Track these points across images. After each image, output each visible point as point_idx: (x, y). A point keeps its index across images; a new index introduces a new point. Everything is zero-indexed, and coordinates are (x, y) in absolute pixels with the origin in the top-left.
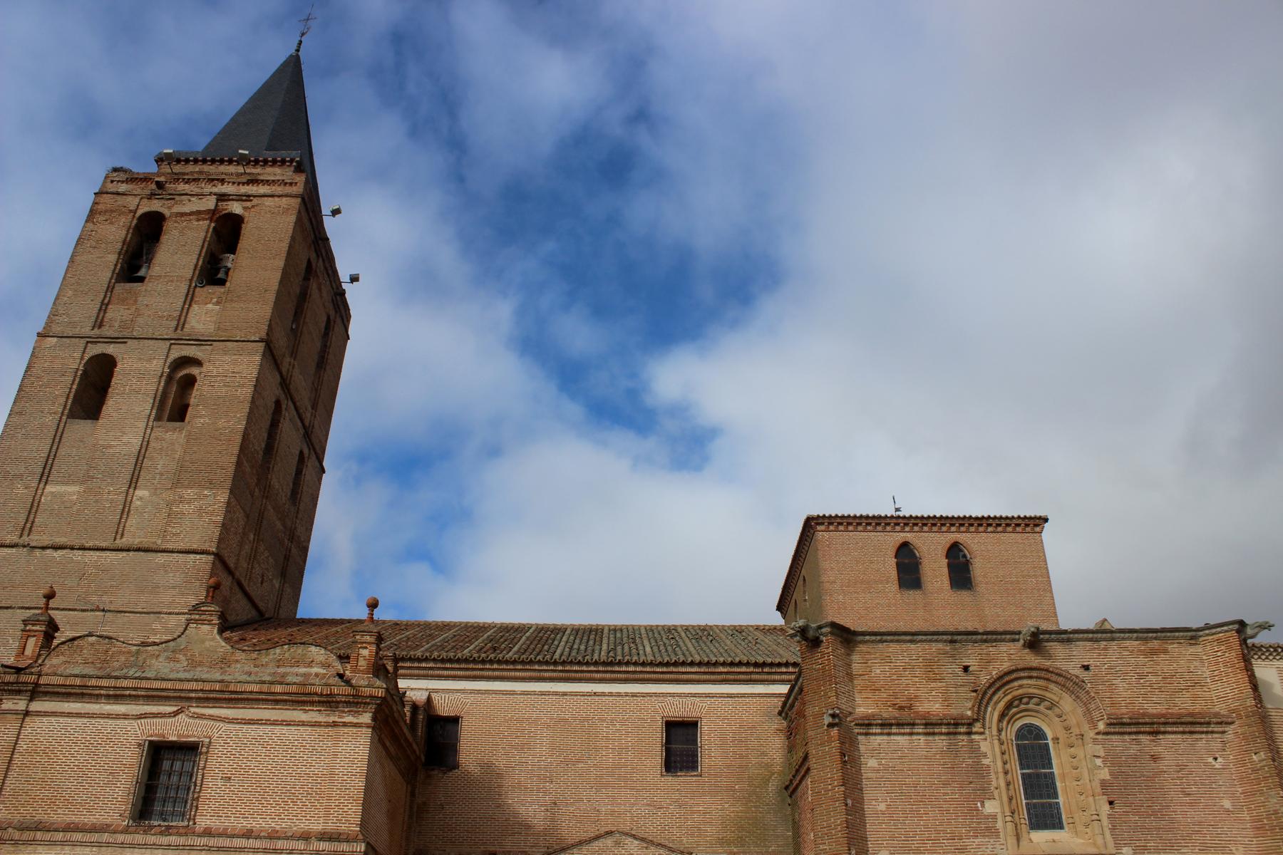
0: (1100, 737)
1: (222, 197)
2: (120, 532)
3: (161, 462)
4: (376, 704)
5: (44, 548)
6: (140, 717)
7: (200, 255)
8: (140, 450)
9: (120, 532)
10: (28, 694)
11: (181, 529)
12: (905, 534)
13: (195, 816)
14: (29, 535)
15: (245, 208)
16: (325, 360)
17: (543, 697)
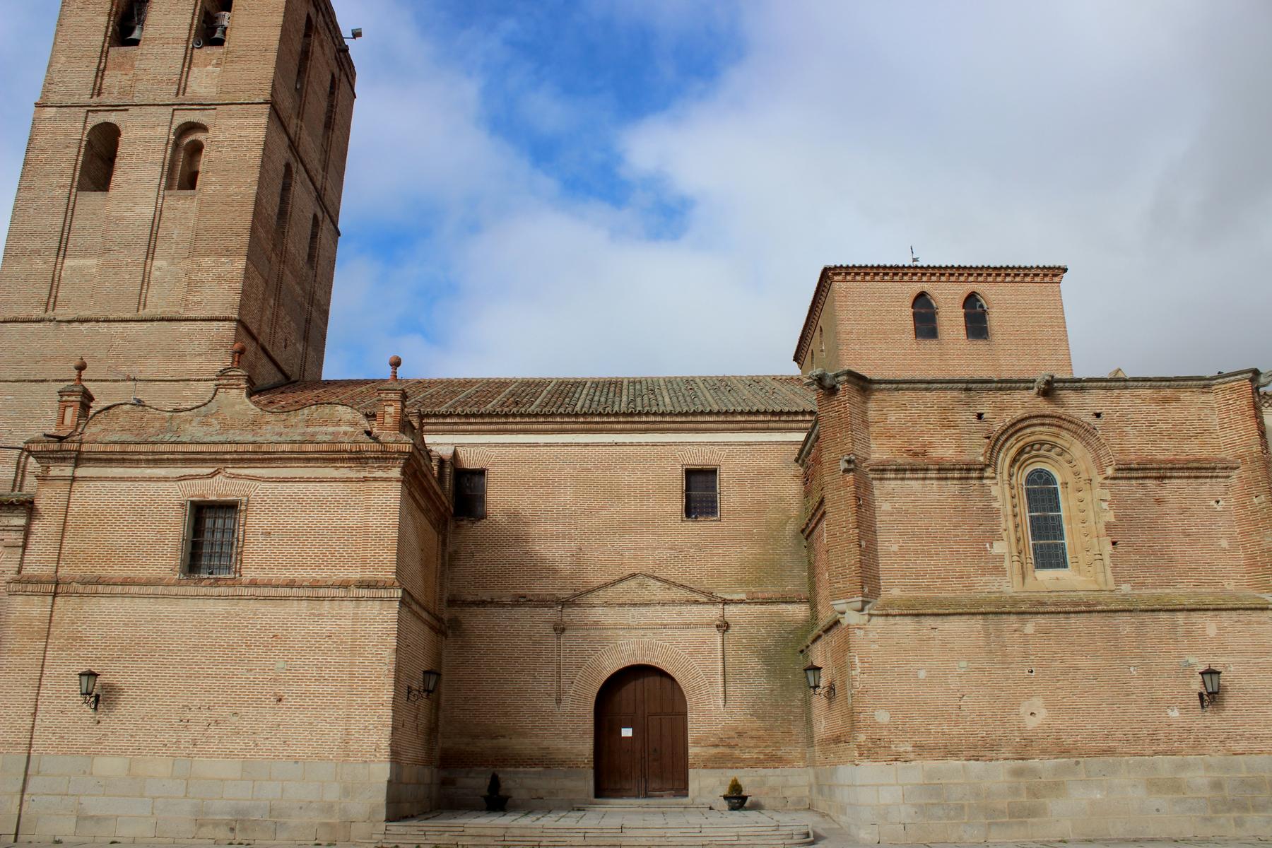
0: (1108, 482)
2: (142, 303)
3: (176, 232)
4: (406, 459)
5: (69, 322)
6: (180, 479)
7: (194, 14)
8: (154, 220)
9: (142, 303)
10: (73, 461)
11: (202, 297)
12: (922, 284)
13: (240, 569)
14: (53, 310)
16: (333, 121)
17: (566, 448)
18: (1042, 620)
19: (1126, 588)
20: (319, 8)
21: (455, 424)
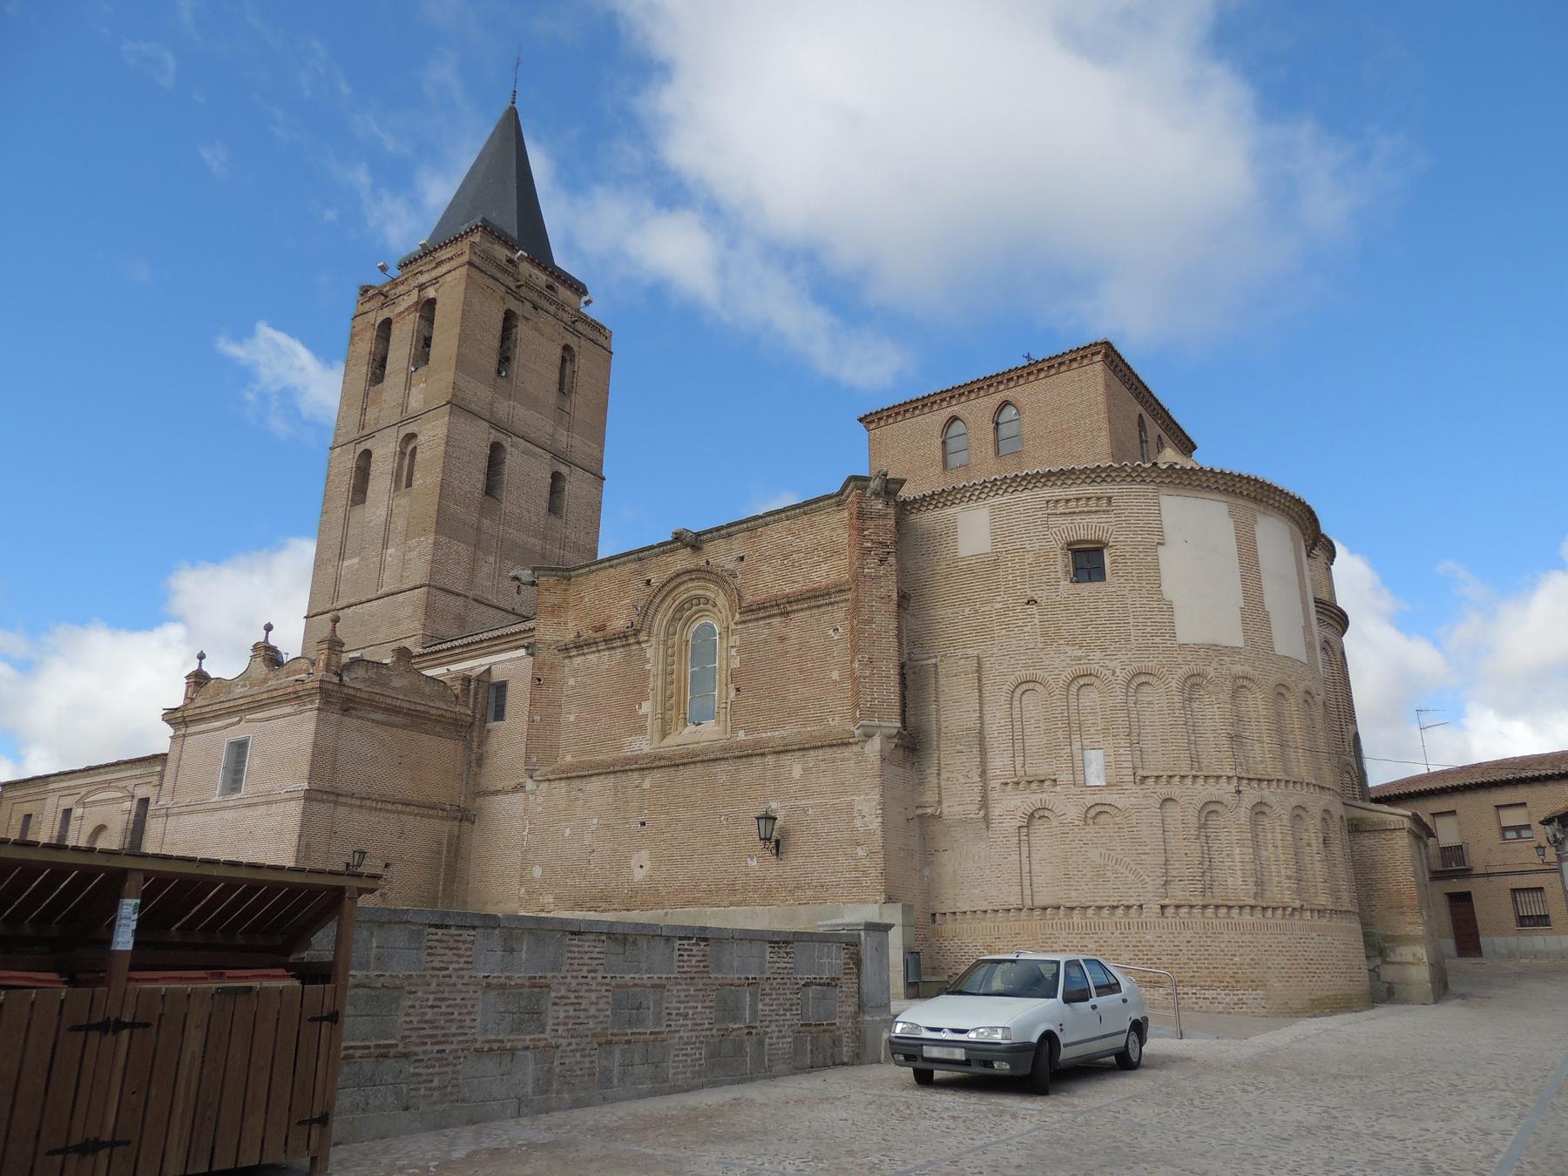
1: (422, 287)
5: (343, 608)
12: (952, 408)
16: (574, 385)
18: (657, 774)
19: (741, 735)
20: (522, 299)
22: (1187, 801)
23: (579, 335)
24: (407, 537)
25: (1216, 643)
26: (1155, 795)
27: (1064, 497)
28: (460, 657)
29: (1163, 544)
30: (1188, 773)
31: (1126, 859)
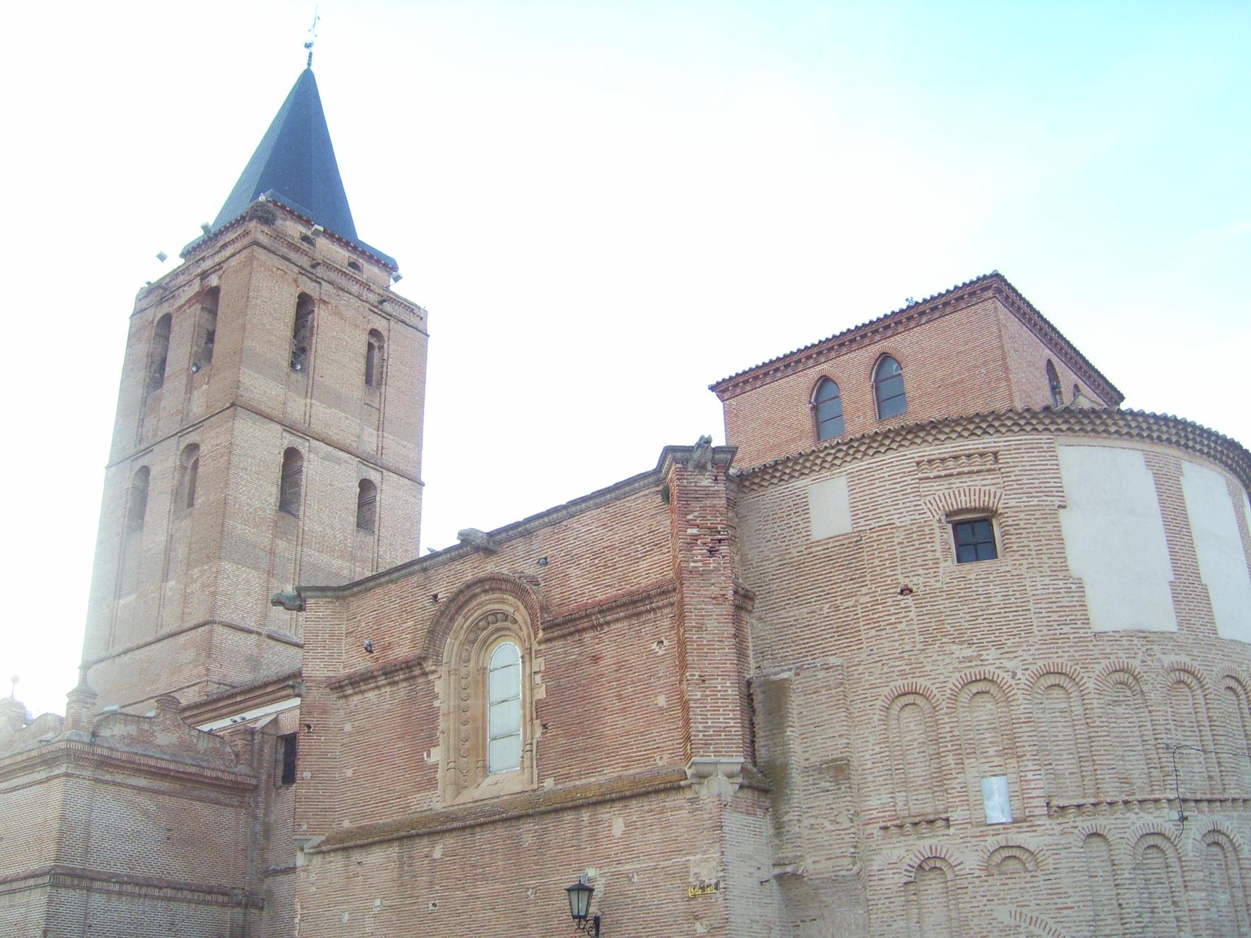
0: (543, 647)
1: (204, 275)
12: (820, 367)
14: (113, 647)
15: (220, 278)
16: (384, 376)
18: (450, 840)
19: (549, 783)
21: (273, 692)
22: (1119, 836)
23: (388, 316)
24: (189, 566)
25: (1142, 628)
26: (1075, 831)
27: (938, 456)
28: (242, 705)
29: (1064, 507)
30: (1116, 799)
31: (1043, 917)
